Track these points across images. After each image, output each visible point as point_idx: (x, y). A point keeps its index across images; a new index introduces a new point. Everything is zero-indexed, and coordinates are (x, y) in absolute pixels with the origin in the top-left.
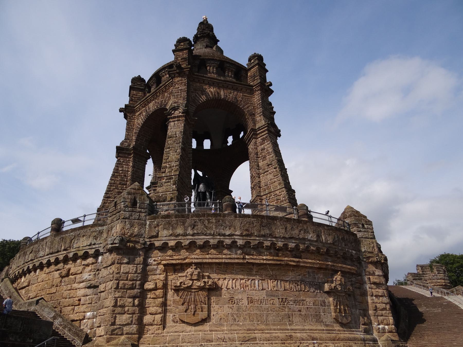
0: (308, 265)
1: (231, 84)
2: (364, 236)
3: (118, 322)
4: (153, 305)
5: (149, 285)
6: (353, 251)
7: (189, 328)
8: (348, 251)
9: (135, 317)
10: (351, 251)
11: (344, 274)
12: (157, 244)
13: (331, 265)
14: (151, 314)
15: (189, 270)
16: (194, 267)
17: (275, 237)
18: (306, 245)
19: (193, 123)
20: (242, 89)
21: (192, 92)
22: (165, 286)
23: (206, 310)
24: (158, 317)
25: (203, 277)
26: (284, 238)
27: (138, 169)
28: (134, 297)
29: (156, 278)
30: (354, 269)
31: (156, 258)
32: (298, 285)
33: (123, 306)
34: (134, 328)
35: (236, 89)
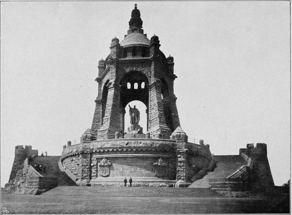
3: (84, 175)
4: (93, 171)
5: (92, 165)
7: (104, 178)
9: (89, 174)
11: (162, 158)
12: (94, 151)
14: (93, 173)
15: (103, 160)
16: (104, 159)
22: (97, 165)
23: (108, 172)
24: (95, 174)
25: (108, 162)
28: (88, 168)
29: (94, 163)
31: (95, 156)
33: (85, 171)
34: (88, 177)
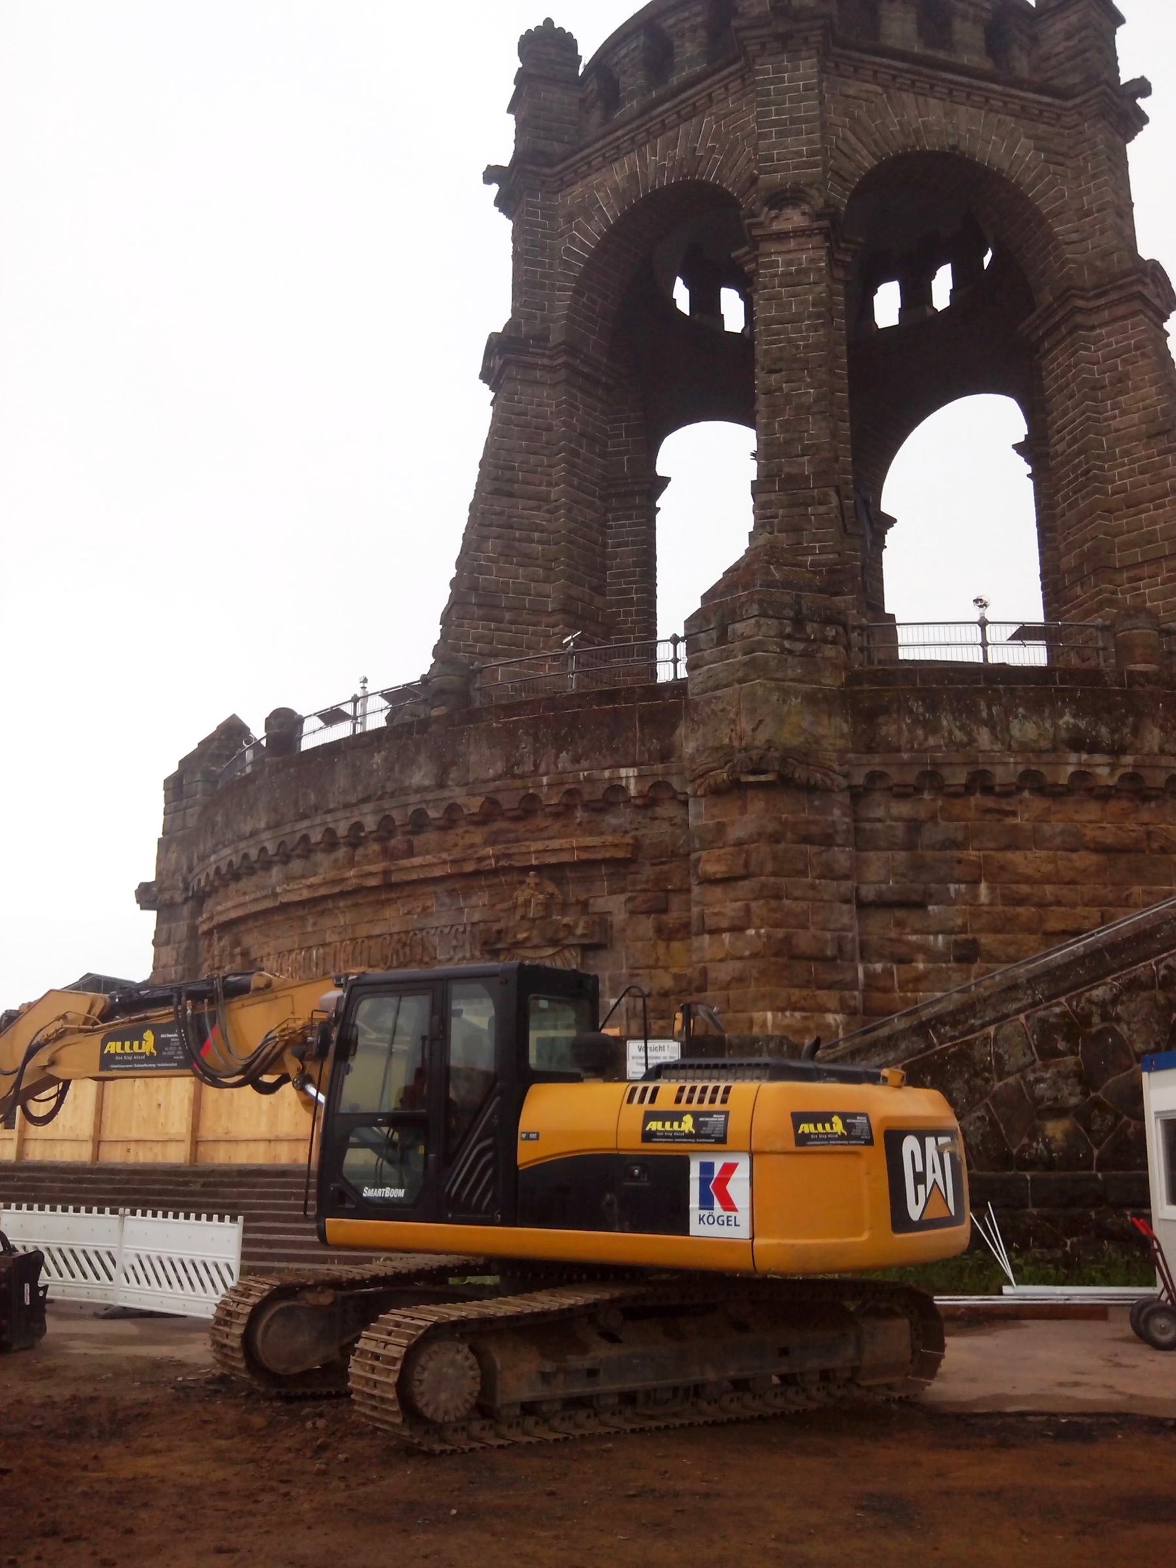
0: (414, 877)
1: (667, 106)
2: (710, 684)
6: (623, 772)
8: (588, 779)
10: (607, 774)
13: (497, 858)
17: (329, 811)
18: (411, 809)
19: (560, 361)
20: (710, 95)
21: (561, 235)
26: (347, 806)
27: (619, 545)
30: (616, 846)
32: (405, 945)
35: (695, 111)
